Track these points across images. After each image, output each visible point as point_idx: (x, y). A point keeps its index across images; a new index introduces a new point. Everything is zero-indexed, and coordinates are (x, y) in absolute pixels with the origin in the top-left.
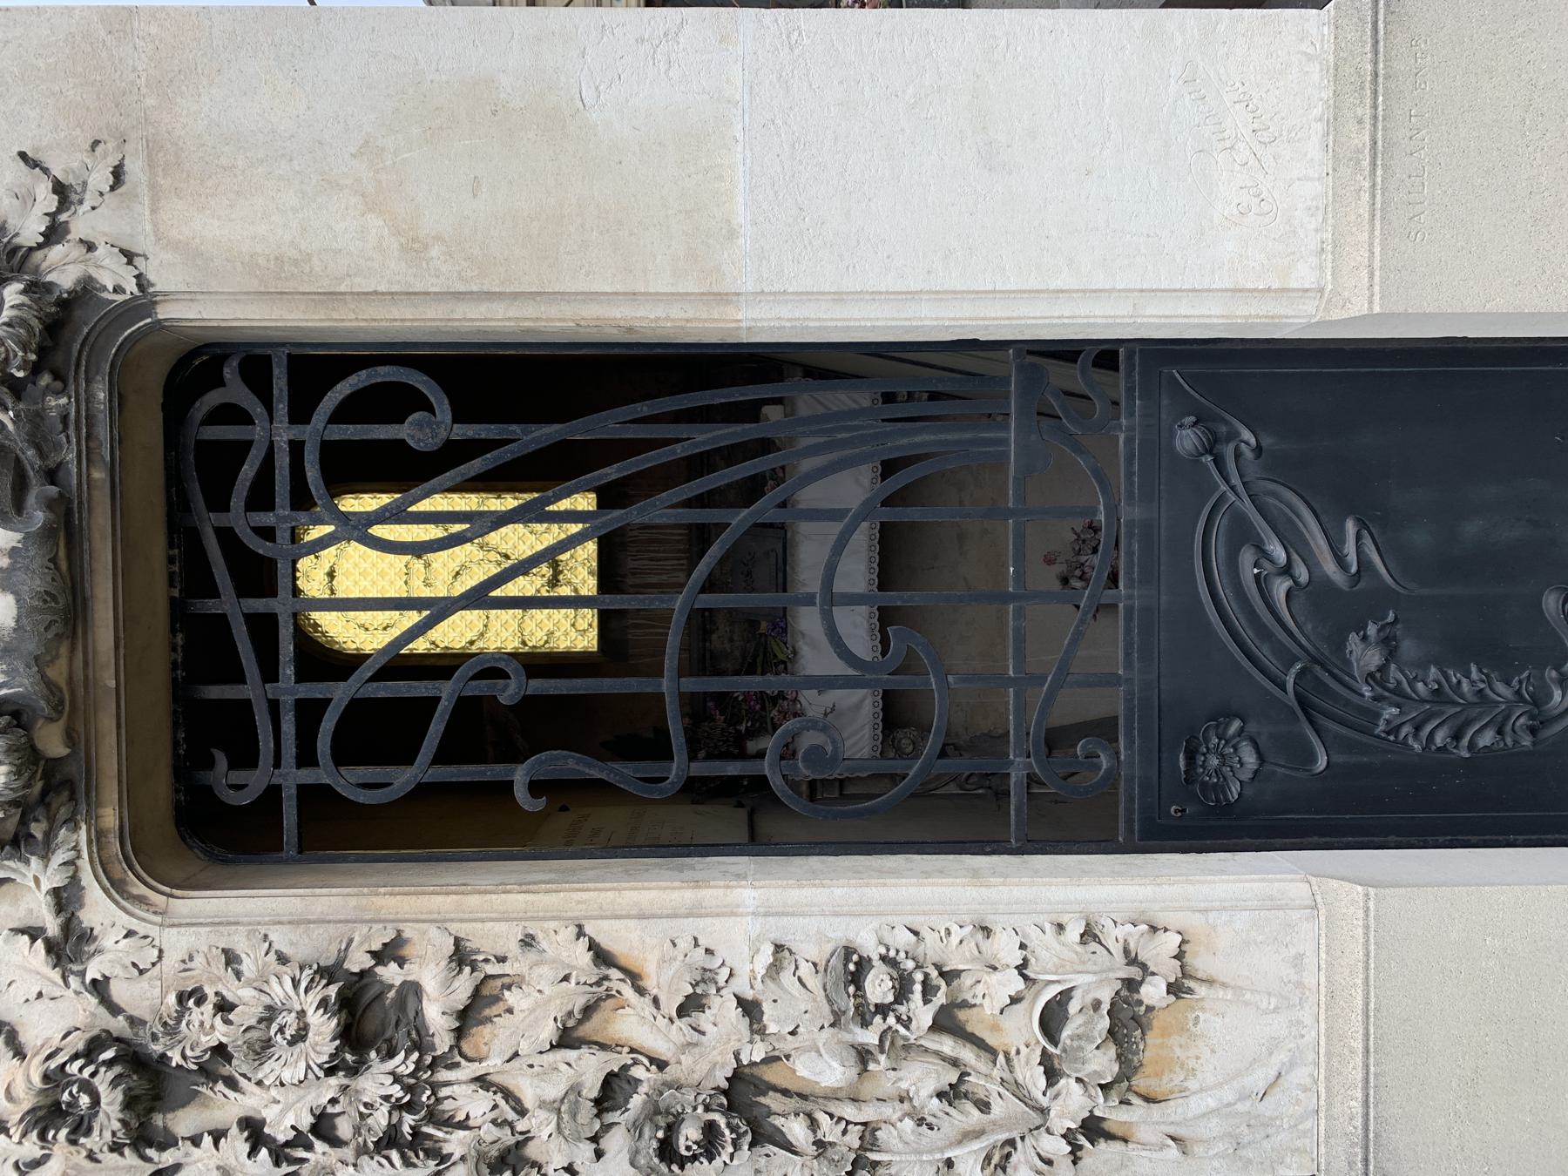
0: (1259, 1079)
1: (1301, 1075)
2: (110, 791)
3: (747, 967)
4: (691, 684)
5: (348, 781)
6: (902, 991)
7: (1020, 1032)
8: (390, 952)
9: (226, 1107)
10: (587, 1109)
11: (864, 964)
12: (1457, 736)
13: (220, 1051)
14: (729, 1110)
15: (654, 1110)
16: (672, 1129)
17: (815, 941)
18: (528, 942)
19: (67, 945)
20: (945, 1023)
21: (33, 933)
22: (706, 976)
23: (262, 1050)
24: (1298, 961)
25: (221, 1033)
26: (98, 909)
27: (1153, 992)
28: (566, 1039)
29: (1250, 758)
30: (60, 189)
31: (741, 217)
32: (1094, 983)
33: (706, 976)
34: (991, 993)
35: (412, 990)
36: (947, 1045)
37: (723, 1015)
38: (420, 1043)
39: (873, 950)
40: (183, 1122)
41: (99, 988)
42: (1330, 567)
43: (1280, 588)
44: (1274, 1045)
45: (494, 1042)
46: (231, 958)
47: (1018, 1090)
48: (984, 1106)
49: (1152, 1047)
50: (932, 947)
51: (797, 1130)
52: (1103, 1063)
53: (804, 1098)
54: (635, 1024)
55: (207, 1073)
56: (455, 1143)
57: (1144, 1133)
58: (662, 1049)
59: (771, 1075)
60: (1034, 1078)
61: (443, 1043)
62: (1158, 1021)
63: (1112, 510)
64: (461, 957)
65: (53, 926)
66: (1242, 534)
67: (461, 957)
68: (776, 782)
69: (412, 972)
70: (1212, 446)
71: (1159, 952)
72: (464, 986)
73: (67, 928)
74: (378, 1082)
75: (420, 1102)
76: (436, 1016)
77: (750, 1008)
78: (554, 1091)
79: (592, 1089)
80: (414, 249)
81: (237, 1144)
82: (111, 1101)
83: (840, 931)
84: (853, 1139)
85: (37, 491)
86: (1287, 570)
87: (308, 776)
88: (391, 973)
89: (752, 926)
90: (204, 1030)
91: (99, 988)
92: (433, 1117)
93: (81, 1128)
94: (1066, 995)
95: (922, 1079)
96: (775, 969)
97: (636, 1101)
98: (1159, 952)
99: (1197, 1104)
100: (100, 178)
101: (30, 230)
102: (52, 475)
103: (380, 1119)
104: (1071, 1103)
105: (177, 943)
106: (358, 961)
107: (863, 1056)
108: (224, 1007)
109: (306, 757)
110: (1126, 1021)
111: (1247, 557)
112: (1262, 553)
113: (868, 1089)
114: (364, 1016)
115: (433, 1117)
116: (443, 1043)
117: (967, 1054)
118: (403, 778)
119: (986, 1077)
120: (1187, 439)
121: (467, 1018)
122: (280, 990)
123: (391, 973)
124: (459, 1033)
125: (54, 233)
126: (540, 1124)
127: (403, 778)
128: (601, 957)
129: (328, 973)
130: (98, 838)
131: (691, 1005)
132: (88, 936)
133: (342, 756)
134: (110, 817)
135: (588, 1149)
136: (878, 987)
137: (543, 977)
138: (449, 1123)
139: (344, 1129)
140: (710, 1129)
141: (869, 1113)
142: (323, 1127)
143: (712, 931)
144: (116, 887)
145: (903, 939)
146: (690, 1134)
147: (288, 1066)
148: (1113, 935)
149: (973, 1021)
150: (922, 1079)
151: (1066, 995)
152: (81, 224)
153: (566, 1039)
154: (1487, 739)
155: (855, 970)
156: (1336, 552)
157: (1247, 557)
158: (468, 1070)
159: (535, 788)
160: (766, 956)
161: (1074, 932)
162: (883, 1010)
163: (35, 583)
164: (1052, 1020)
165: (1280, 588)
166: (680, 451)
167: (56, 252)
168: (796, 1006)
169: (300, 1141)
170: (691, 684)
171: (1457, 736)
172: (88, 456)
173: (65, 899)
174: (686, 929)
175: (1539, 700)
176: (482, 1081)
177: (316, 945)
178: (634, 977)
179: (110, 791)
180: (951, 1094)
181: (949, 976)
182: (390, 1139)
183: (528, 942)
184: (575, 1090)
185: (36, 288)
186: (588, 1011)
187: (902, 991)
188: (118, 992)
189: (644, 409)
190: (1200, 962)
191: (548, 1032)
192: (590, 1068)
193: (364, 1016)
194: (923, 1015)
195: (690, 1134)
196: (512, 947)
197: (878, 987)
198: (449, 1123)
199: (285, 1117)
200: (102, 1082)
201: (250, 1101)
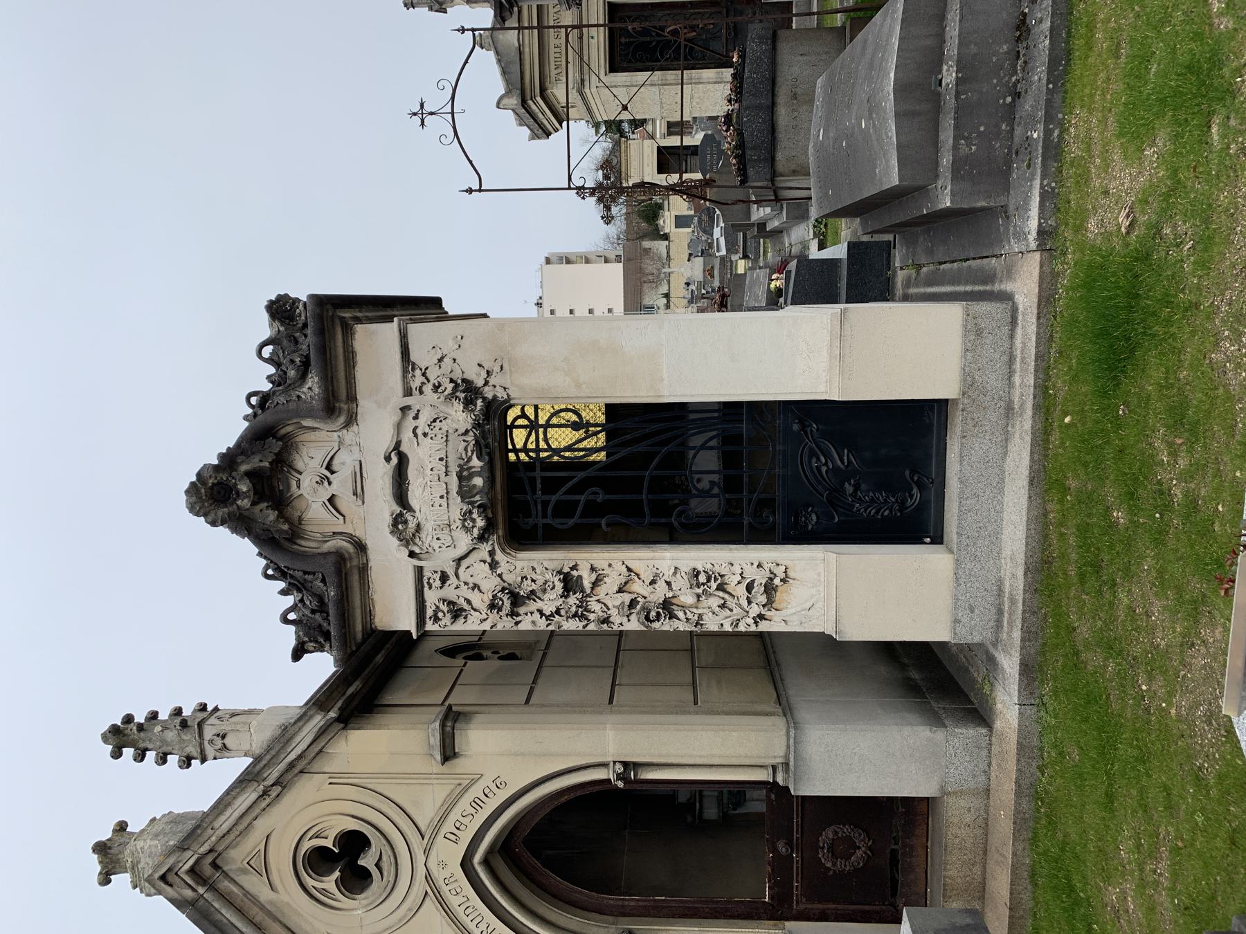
0: (808, 605)
1: (820, 604)
2: (501, 526)
3: (668, 573)
4: (650, 497)
5: (556, 523)
6: (709, 580)
7: (741, 591)
8: (574, 568)
9: (533, 606)
10: (626, 608)
11: (699, 573)
12: (877, 513)
13: (533, 592)
14: (663, 609)
15: (643, 608)
16: (648, 613)
17: (686, 567)
18: (610, 565)
19: (493, 565)
20: (721, 588)
21: (485, 562)
22: (657, 575)
23: (544, 591)
24: (819, 574)
25: (534, 587)
26: (499, 556)
27: (777, 581)
28: (620, 591)
29: (814, 517)
30: (488, 372)
31: (665, 375)
32: (761, 578)
33: (657, 575)
34: (732, 581)
35: (580, 577)
36: (721, 594)
37: (661, 585)
38: (583, 591)
39: (701, 569)
40: (522, 610)
41: (500, 576)
42: (839, 463)
43: (824, 469)
44: (812, 597)
45: (601, 591)
46: (534, 569)
47: (740, 606)
48: (731, 610)
49: (778, 596)
50: (717, 569)
51: (681, 614)
52: (763, 599)
53: (683, 607)
54: (638, 587)
55: (528, 598)
56: (592, 617)
57: (775, 619)
58: (646, 594)
59: (674, 601)
60: (745, 603)
61: (588, 591)
62: (780, 589)
63: (774, 447)
64: (593, 569)
65: (489, 560)
66: (812, 454)
67: (593, 569)
68: (676, 524)
69: (580, 573)
70: (803, 427)
71: (780, 571)
72: (594, 576)
73: (493, 560)
74: (573, 600)
75: (583, 604)
76: (587, 584)
77: (668, 584)
78: (617, 603)
79: (627, 603)
80: (578, 386)
81: (537, 615)
82: (507, 603)
83: (692, 564)
84: (696, 617)
85: (484, 451)
86: (826, 464)
87: (545, 521)
88: (574, 573)
89: (669, 562)
90: (527, 587)
91: (500, 576)
92: (586, 610)
93: (500, 610)
94: (753, 581)
95: (714, 602)
96: (675, 573)
97: (639, 607)
98: (780, 571)
99: (790, 611)
100: (497, 369)
101: (479, 382)
102: (487, 446)
103: (574, 609)
104: (755, 610)
105: (519, 564)
106: (566, 570)
107: (698, 596)
108: (533, 581)
109: (545, 516)
110: (769, 589)
111: (814, 460)
112: (818, 459)
113: (700, 605)
114: (570, 584)
115: (586, 610)
116: (588, 591)
117: (726, 596)
118: (571, 522)
119: (731, 603)
120: (796, 427)
121: (595, 584)
122: (548, 576)
123: (574, 573)
124: (592, 589)
125: (486, 383)
126: (614, 612)
127: (571, 522)
128: (629, 570)
129: (560, 572)
130: (498, 538)
131: (653, 582)
132: (497, 563)
133: (554, 516)
134: (501, 532)
135: (625, 619)
136: (702, 578)
137: (614, 574)
138: (589, 611)
139: (563, 612)
140: (658, 613)
141: (700, 611)
142: (558, 612)
143: (657, 563)
144: (503, 550)
145: (709, 566)
146: (653, 614)
147: (551, 595)
148: (766, 566)
149: (729, 588)
150: (714, 602)
151: (753, 581)
152: (492, 381)
153: (620, 591)
154: (886, 513)
155: (696, 574)
156: (841, 459)
157: (814, 460)
158: (595, 598)
159: (608, 525)
160: (672, 570)
161: (756, 565)
162: (703, 584)
163: (486, 474)
164: (749, 588)
165: (824, 469)
166: (649, 442)
167: (486, 389)
168: (681, 583)
169: (552, 615)
170: (650, 497)
171: (877, 513)
172: (495, 440)
173: (492, 553)
174: (651, 563)
175: (903, 502)
176: (598, 601)
177: (555, 565)
178: (638, 575)
179: (501, 526)
180: (723, 606)
181: (722, 576)
182: (576, 615)
183: (610, 565)
184: (623, 603)
185: (484, 399)
186: (626, 583)
187: (709, 580)
188: (504, 577)
189: (637, 419)
190: (791, 574)
191: (616, 588)
192: (627, 598)
193: (570, 584)
194: (714, 585)
195: (653, 614)
196: (606, 567)
197: (702, 578)
198: (589, 611)
199: (549, 609)
200: (505, 599)
201: (539, 604)
